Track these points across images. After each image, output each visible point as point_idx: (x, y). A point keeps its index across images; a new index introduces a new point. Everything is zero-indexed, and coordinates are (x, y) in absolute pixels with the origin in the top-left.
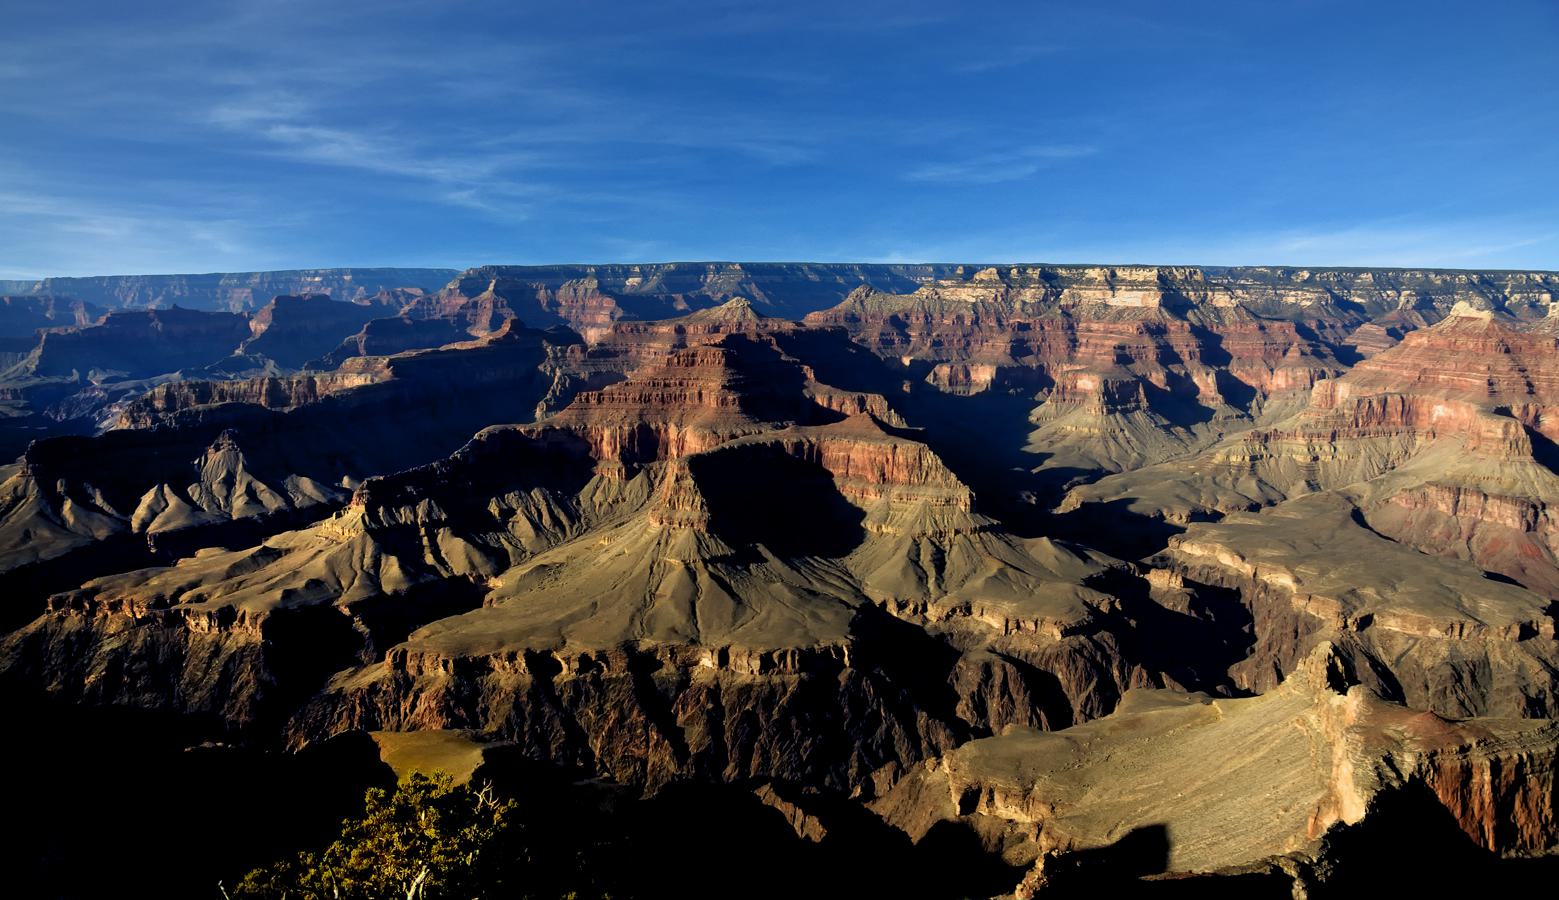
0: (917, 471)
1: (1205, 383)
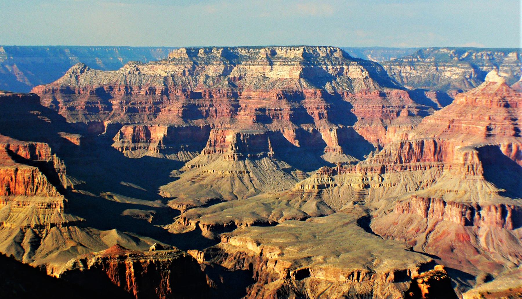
0: (30, 186)
1: (329, 136)
